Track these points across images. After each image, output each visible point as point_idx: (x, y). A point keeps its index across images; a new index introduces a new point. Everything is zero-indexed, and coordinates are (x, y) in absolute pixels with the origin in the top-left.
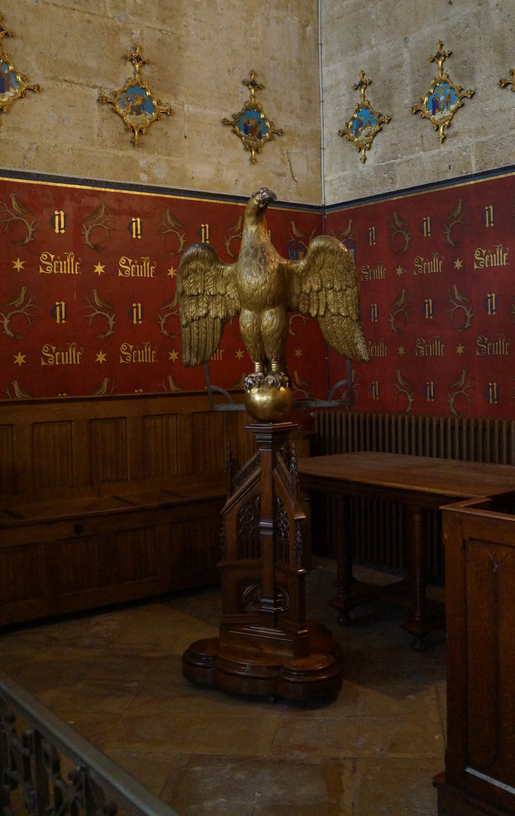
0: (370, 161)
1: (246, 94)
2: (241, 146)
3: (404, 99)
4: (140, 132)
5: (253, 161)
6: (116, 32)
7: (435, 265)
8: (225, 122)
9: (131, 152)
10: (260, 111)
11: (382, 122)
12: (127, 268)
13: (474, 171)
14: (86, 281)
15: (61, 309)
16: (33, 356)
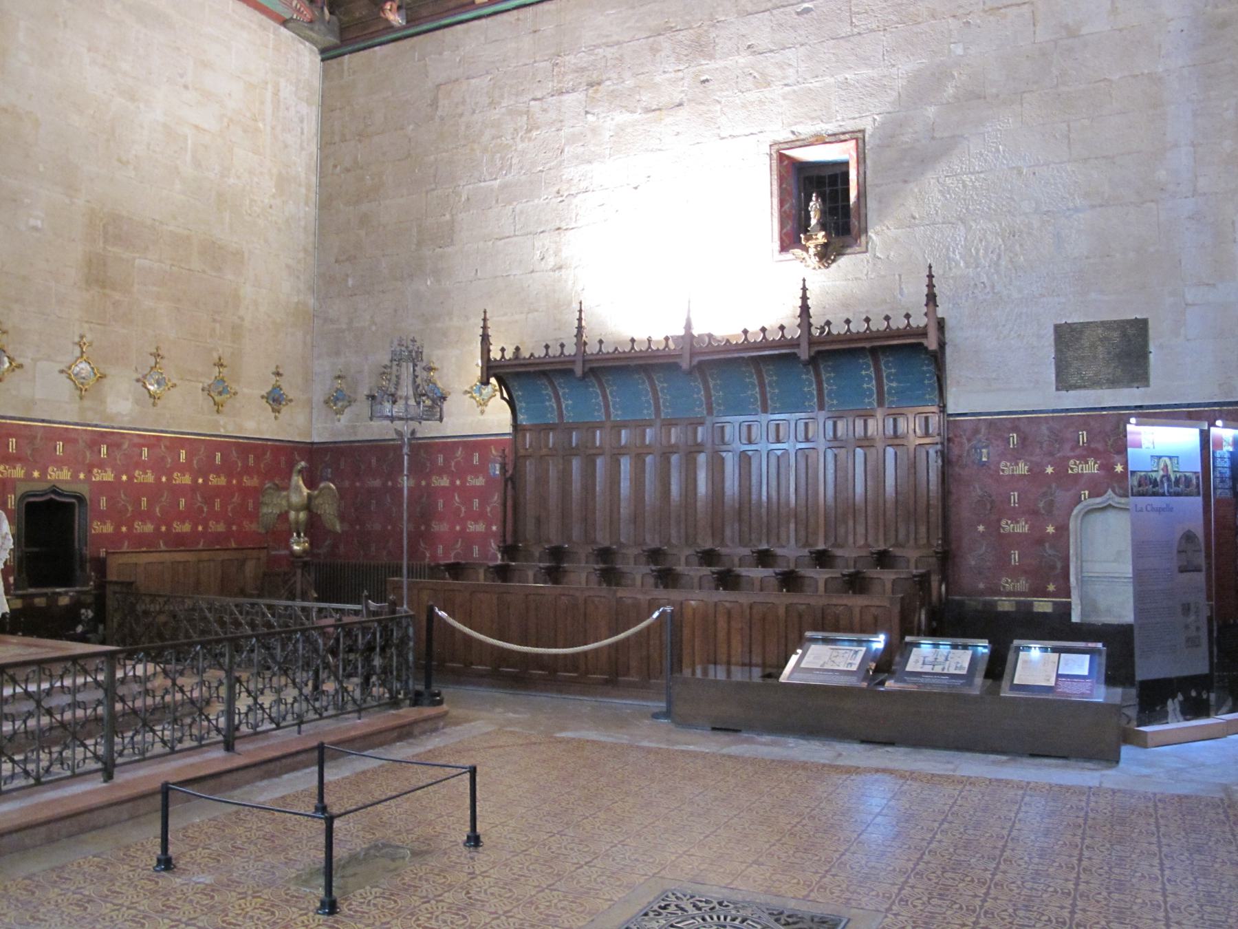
0: (342, 421)
1: (273, 379)
7: (377, 483)
8: (263, 397)
9: (217, 417)
12: (214, 480)
14: (194, 487)
16: (169, 526)
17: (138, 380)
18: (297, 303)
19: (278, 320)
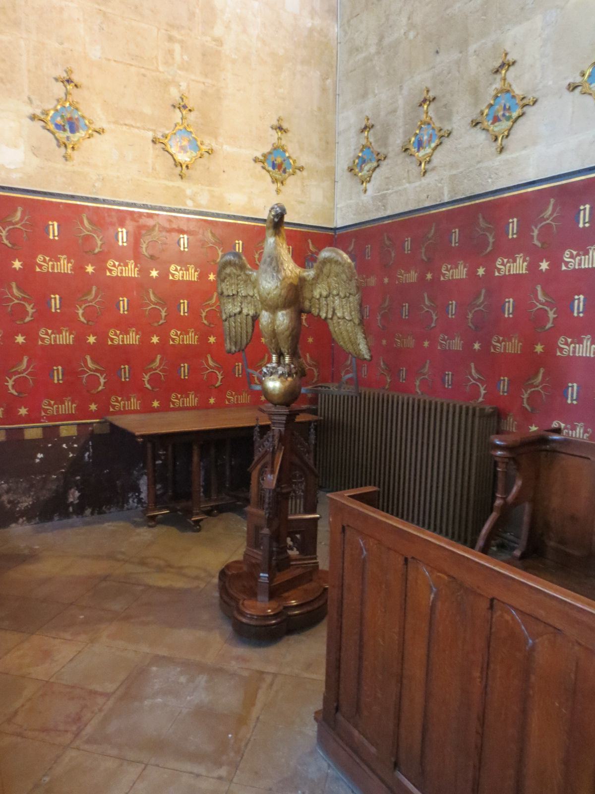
0: (369, 192)
1: (274, 136)
2: (269, 179)
3: (397, 140)
4: (187, 167)
5: (278, 191)
6: (166, 84)
7: (412, 276)
8: (256, 160)
9: (179, 183)
10: (285, 151)
11: (380, 160)
13: (446, 199)
15: (124, 304)
17: (33, 118)
18: (311, 30)
19: (281, 52)
